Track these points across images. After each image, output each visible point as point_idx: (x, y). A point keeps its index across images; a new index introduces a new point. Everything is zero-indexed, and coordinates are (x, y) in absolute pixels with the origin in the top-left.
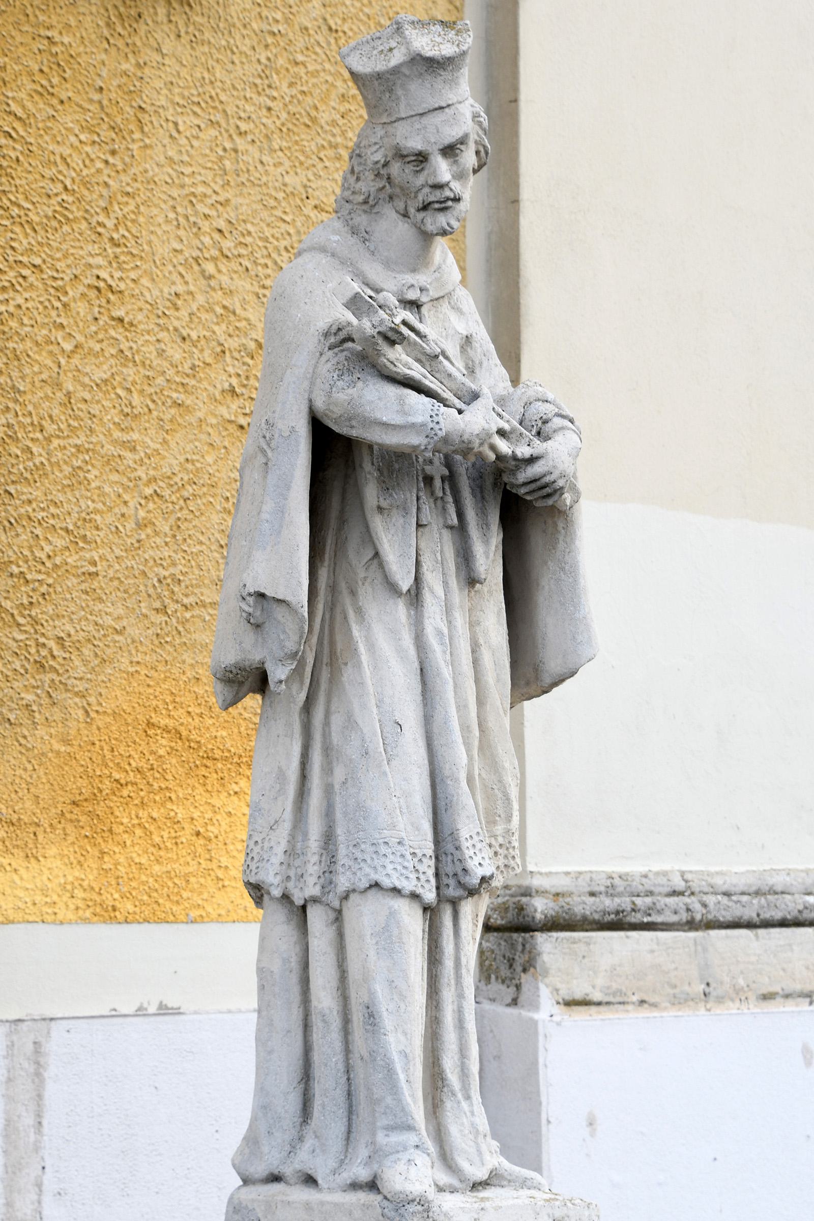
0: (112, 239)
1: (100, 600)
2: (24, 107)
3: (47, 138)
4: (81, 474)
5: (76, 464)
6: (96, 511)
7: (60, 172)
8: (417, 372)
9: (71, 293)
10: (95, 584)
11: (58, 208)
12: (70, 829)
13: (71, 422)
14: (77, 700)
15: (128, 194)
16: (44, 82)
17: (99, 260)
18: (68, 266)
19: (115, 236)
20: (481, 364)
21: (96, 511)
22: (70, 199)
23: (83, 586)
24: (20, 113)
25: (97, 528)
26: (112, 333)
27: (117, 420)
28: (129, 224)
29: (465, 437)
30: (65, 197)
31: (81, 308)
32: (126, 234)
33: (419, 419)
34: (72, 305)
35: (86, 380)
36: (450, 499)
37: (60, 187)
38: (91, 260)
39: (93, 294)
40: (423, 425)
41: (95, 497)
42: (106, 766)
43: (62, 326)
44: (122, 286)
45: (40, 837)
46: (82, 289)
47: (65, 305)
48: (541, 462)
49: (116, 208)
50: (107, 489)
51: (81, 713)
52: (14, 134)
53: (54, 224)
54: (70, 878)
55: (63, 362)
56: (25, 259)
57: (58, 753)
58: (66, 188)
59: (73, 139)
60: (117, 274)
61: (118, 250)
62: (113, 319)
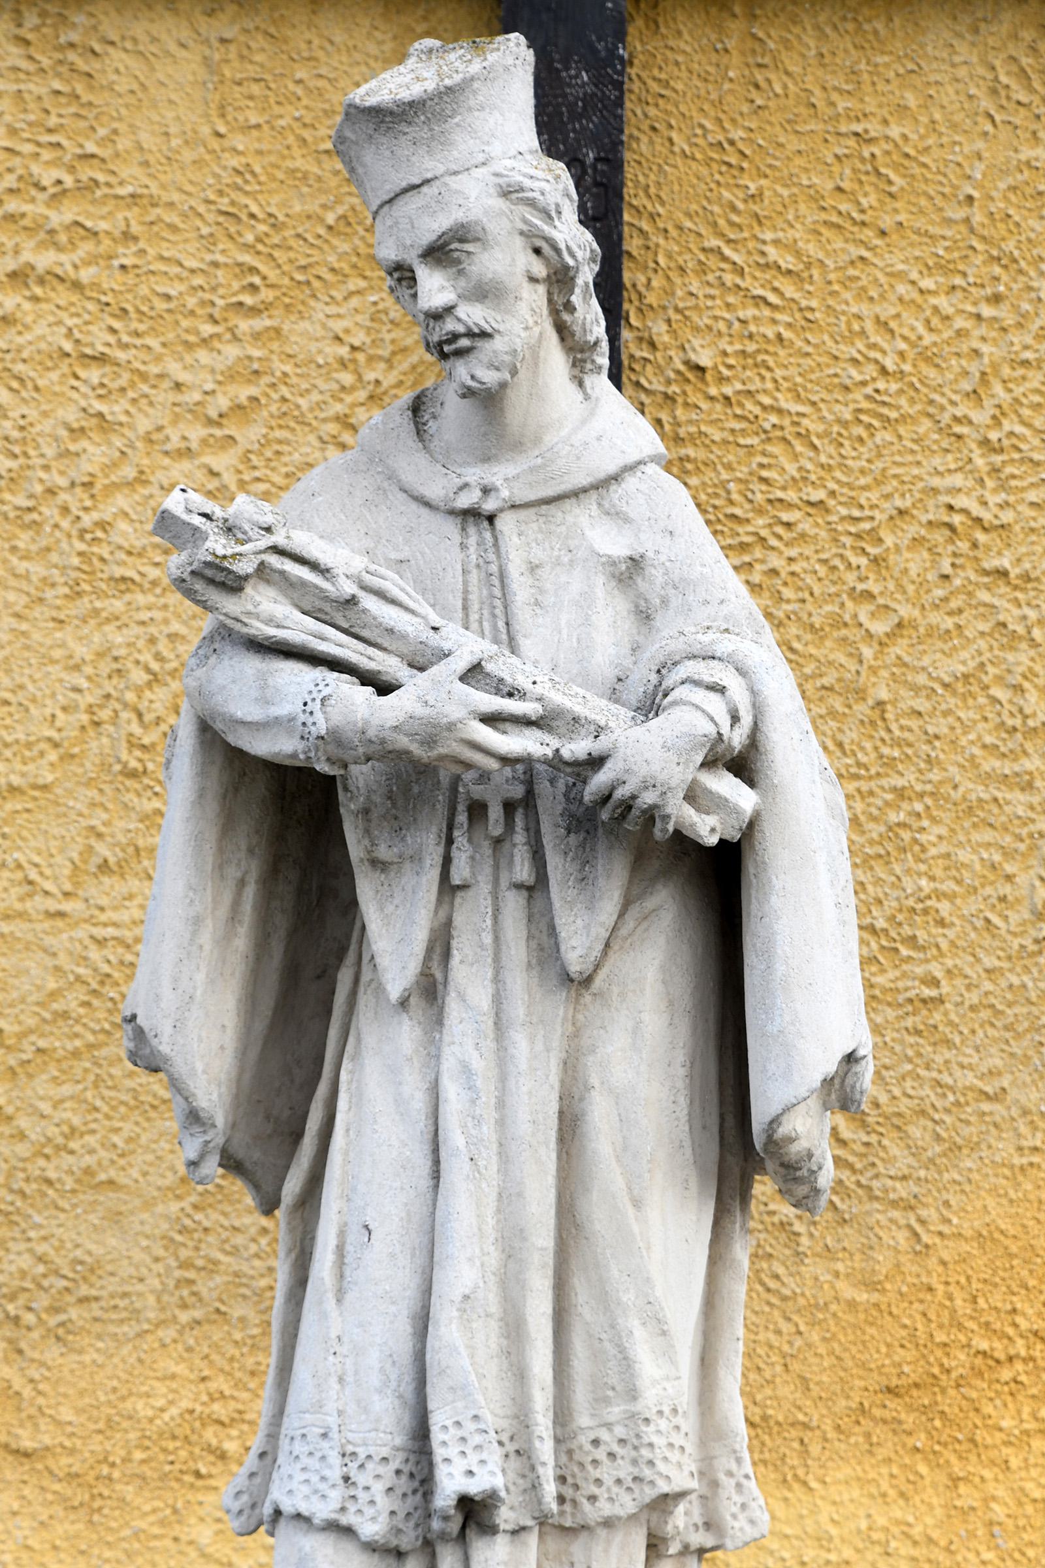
0: (985, 442)
1: (949, 1043)
2: (798, 254)
3: (847, 295)
4: (906, 835)
5: (893, 817)
6: (940, 895)
7: (873, 346)
9: (889, 541)
10: (937, 1017)
11: (865, 405)
12: (879, 1433)
13: (886, 751)
14: (895, 1214)
15: (1025, 363)
16: (844, 207)
17: (958, 480)
18: (887, 497)
19: (993, 436)
21: (940, 895)
22: (894, 387)
23: (909, 1022)
24: (788, 261)
25: (941, 923)
26: (984, 596)
27: (988, 740)
28: (1026, 412)
30: (881, 385)
31: (915, 563)
32: (1019, 429)
34: (892, 558)
35: (922, 679)
37: (871, 370)
38: (936, 482)
39: (939, 536)
41: (938, 872)
42: (960, 1327)
43: (869, 596)
44: (1007, 517)
45: (815, 1449)
46: (913, 530)
47: (875, 561)
49: (998, 389)
50: (964, 856)
51: (902, 1237)
52: (773, 298)
53: (860, 431)
54: (881, 1521)
55: (867, 652)
56: (791, 496)
57: (852, 1305)
58: (884, 371)
59: (902, 289)
60: (993, 499)
61: (998, 459)
62: (986, 573)
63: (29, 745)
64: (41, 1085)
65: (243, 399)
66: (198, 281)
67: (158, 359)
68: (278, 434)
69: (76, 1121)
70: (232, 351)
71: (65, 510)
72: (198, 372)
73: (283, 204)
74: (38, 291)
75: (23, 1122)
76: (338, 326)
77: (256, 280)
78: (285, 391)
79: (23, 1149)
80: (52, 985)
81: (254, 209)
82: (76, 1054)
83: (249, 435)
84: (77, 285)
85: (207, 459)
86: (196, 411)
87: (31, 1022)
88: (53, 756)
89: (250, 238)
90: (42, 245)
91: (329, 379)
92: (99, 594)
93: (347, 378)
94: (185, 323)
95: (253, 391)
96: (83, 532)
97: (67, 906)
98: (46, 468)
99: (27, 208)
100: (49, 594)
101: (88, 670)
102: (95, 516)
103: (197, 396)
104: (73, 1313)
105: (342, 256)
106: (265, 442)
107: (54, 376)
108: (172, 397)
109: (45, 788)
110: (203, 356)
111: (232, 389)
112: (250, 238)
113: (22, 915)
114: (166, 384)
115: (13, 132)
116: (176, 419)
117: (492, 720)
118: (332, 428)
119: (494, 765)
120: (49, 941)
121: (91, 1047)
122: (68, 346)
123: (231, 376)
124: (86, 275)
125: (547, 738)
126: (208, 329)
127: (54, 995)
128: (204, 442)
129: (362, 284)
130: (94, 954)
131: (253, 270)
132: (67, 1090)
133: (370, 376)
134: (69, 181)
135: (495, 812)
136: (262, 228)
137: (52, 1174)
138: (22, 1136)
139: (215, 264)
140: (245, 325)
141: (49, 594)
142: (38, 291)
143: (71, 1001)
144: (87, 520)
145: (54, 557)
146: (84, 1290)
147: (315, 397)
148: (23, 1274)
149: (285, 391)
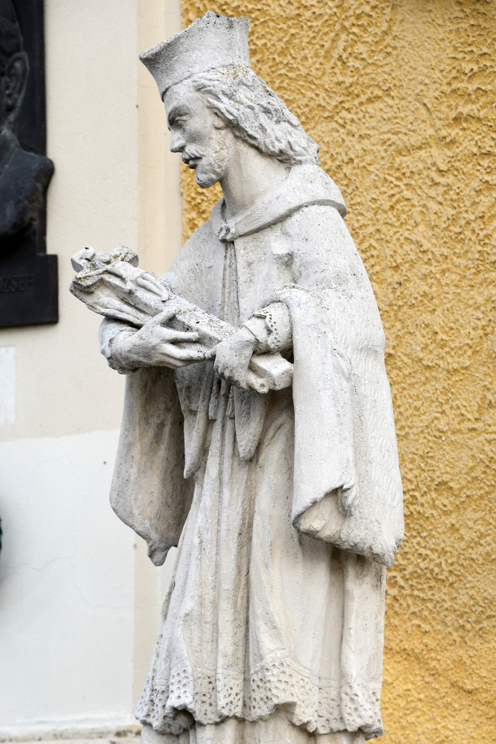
63: (460, 348)
64: (469, 514)
69: (483, 530)
71: (473, 231)
74: (465, 125)
75: (463, 531)
79: (463, 545)
80: (471, 464)
82: (481, 497)
84: (479, 119)
87: (464, 483)
88: (469, 353)
90: (466, 102)
92: (487, 271)
96: (480, 240)
97: (476, 425)
98: (467, 211)
99: (461, 85)
100: (468, 273)
101: (483, 309)
102: (485, 232)
104: (485, 624)
107: (470, 166)
109: (466, 368)
113: (459, 431)
115: (456, 48)
120: (470, 443)
121: (487, 493)
122: (475, 150)
124: (482, 114)
127: (472, 469)
130: (487, 448)
132: (479, 515)
134: (476, 68)
137: (474, 556)
138: (462, 538)
141: (468, 273)
142: (465, 125)
143: (478, 473)
144: (482, 234)
145: (470, 255)
146: (489, 612)
148: (465, 605)
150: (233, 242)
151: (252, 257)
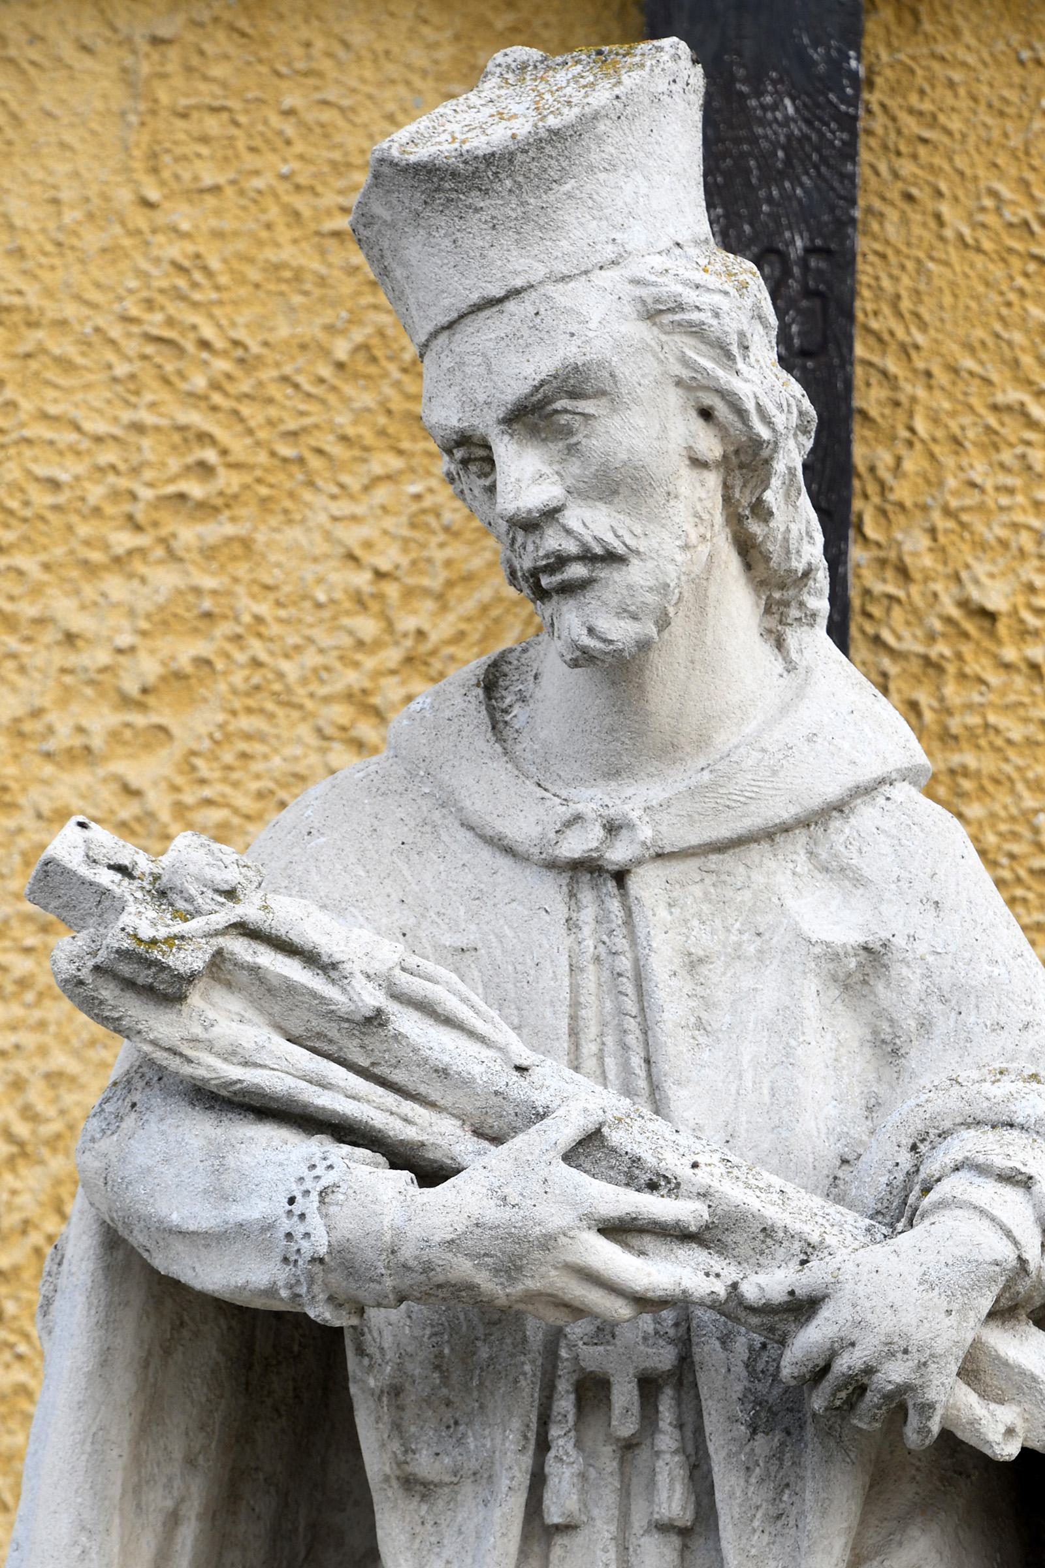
8: (285, 1069)
20: (925, 1025)
29: (408, 1253)
33: (252, 1210)
36: (667, 1440)
40: (268, 1227)
48: (825, 1312)
65: (184, 662)
66: (108, 456)
67: (37, 591)
68: (246, 723)
70: (166, 579)
72: (107, 616)
73: (259, 324)
76: (352, 536)
77: (210, 455)
78: (257, 648)
81: (208, 332)
83: (194, 724)
85: (121, 767)
86: (100, 682)
89: (199, 382)
91: (335, 627)
93: (368, 627)
94: (84, 530)
95: (202, 648)
103: (103, 657)
105: (360, 415)
106: (223, 737)
108: (60, 657)
110: (115, 586)
111: (165, 644)
112: (199, 382)
114: (50, 635)
116: (66, 696)
117: (619, 1230)
118: (340, 713)
119: (622, 1310)
123: (164, 621)
125: (716, 1263)
126: (124, 540)
128: (114, 736)
129: (396, 463)
131: (205, 438)
133: (408, 623)
135: (624, 1395)
136: (222, 365)
139: (139, 428)
140: (188, 534)
147: (311, 658)
149: (257, 648)
150: (620, 877)
151: (703, 940)
